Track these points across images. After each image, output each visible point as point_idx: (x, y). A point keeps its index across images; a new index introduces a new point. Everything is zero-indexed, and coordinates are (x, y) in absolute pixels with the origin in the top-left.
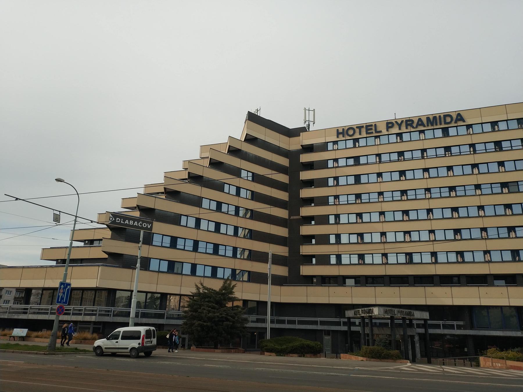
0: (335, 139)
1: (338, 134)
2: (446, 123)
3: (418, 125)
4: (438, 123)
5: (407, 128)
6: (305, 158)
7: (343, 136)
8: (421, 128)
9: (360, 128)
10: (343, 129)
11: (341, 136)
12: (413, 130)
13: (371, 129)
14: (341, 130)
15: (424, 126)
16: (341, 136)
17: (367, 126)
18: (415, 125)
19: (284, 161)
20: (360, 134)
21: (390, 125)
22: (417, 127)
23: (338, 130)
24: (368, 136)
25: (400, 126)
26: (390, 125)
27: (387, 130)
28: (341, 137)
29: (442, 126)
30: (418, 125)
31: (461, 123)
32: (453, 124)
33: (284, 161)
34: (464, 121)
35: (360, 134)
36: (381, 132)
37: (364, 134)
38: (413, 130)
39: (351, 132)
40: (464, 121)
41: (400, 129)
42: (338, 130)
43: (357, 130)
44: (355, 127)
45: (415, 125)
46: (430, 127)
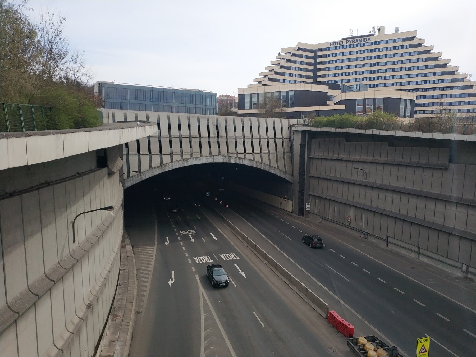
0: (329, 46)
1: (330, 44)
2: (365, 41)
3: (356, 42)
4: (362, 41)
5: (353, 43)
6: (319, 53)
7: (332, 45)
8: (357, 43)
9: (337, 42)
10: (332, 43)
11: (331, 45)
12: (354, 43)
13: (341, 43)
14: (331, 43)
15: (358, 42)
16: (331, 45)
17: (340, 42)
18: (355, 42)
19: (312, 55)
20: (337, 45)
21: (347, 41)
22: (356, 42)
23: (330, 43)
24: (340, 45)
25: (350, 42)
26: (347, 41)
27: (346, 44)
28: (331, 46)
29: (364, 42)
30: (356, 42)
31: (369, 41)
32: (367, 42)
33: (312, 55)
34: (370, 41)
35: (337, 45)
36: (344, 44)
37: (339, 45)
38: (354, 43)
39: (334, 44)
40: (370, 41)
41: (350, 43)
42: (330, 43)
43: (337, 43)
44: (336, 42)
45: (355, 42)
46: (360, 43)
